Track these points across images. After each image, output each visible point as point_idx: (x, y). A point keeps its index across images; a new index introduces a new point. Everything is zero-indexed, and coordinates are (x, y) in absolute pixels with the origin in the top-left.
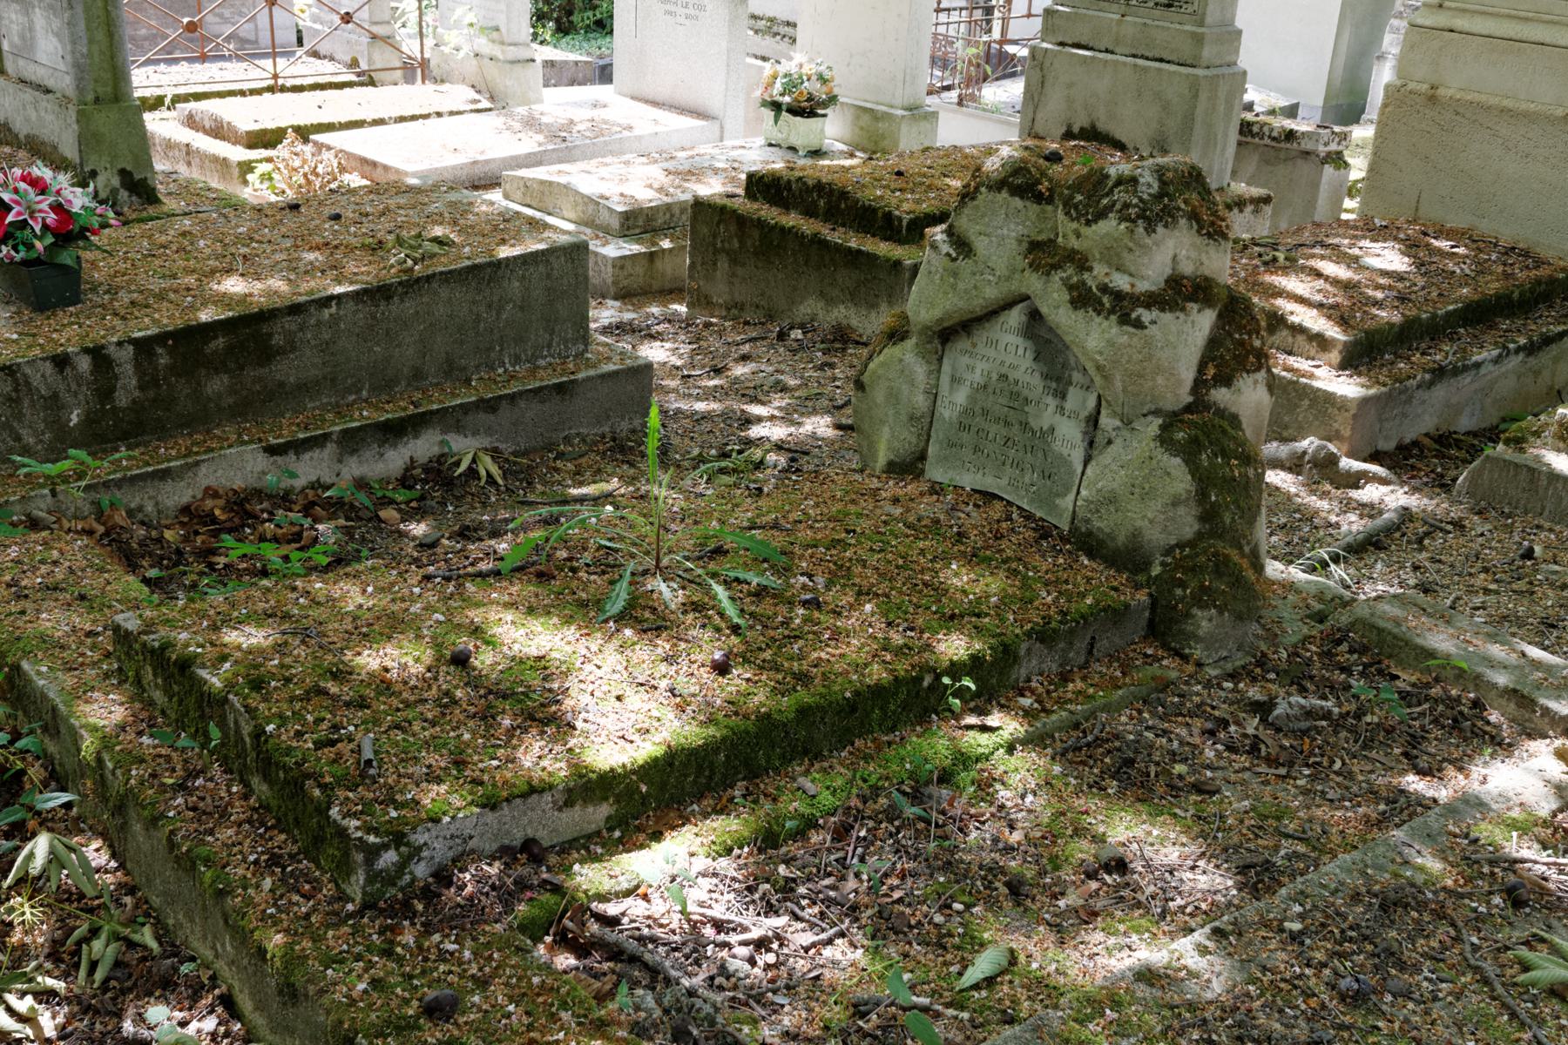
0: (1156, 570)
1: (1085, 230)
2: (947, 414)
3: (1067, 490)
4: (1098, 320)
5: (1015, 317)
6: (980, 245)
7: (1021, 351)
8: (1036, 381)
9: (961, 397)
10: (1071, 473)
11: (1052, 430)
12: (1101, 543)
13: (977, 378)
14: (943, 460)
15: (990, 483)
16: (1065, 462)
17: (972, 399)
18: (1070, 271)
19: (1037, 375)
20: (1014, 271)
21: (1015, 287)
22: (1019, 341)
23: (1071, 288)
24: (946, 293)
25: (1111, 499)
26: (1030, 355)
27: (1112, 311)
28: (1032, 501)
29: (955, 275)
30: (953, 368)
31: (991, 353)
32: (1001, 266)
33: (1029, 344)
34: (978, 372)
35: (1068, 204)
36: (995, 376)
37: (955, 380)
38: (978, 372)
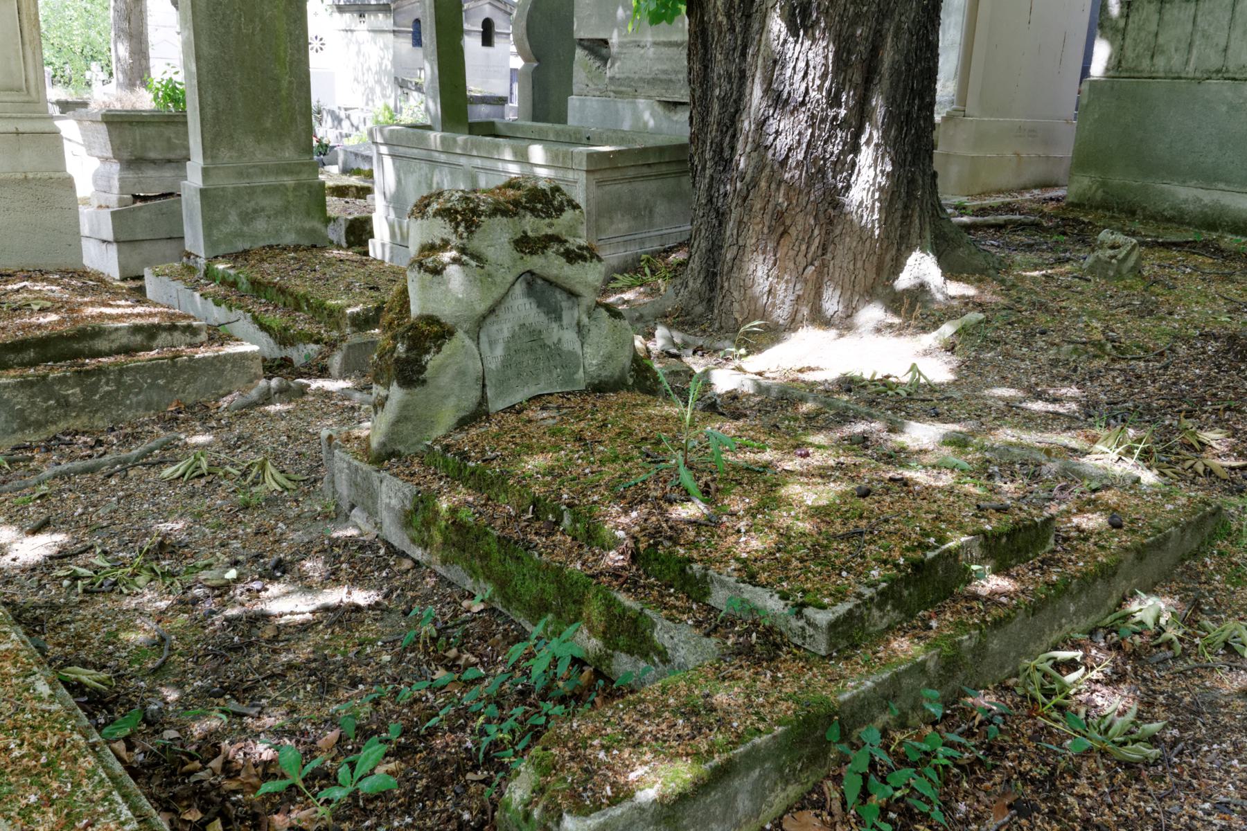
0: (630, 381)
1: (555, 221)
2: (493, 367)
3: (578, 367)
4: (587, 264)
5: (519, 288)
6: (490, 253)
7: (528, 306)
8: (542, 318)
9: (499, 351)
10: (577, 357)
11: (560, 340)
12: (607, 383)
13: (506, 333)
14: (498, 396)
15: (533, 390)
16: (572, 353)
17: (507, 349)
18: (556, 246)
19: (542, 315)
20: (515, 261)
21: (521, 269)
22: (526, 300)
23: (562, 255)
24: (489, 289)
25: (610, 357)
26: (534, 306)
27: (592, 257)
28: (561, 385)
29: (489, 275)
30: (488, 336)
31: (511, 315)
32: (507, 262)
33: (532, 300)
34: (505, 330)
35: (533, 211)
36: (517, 328)
37: (492, 344)
38: (505, 330)
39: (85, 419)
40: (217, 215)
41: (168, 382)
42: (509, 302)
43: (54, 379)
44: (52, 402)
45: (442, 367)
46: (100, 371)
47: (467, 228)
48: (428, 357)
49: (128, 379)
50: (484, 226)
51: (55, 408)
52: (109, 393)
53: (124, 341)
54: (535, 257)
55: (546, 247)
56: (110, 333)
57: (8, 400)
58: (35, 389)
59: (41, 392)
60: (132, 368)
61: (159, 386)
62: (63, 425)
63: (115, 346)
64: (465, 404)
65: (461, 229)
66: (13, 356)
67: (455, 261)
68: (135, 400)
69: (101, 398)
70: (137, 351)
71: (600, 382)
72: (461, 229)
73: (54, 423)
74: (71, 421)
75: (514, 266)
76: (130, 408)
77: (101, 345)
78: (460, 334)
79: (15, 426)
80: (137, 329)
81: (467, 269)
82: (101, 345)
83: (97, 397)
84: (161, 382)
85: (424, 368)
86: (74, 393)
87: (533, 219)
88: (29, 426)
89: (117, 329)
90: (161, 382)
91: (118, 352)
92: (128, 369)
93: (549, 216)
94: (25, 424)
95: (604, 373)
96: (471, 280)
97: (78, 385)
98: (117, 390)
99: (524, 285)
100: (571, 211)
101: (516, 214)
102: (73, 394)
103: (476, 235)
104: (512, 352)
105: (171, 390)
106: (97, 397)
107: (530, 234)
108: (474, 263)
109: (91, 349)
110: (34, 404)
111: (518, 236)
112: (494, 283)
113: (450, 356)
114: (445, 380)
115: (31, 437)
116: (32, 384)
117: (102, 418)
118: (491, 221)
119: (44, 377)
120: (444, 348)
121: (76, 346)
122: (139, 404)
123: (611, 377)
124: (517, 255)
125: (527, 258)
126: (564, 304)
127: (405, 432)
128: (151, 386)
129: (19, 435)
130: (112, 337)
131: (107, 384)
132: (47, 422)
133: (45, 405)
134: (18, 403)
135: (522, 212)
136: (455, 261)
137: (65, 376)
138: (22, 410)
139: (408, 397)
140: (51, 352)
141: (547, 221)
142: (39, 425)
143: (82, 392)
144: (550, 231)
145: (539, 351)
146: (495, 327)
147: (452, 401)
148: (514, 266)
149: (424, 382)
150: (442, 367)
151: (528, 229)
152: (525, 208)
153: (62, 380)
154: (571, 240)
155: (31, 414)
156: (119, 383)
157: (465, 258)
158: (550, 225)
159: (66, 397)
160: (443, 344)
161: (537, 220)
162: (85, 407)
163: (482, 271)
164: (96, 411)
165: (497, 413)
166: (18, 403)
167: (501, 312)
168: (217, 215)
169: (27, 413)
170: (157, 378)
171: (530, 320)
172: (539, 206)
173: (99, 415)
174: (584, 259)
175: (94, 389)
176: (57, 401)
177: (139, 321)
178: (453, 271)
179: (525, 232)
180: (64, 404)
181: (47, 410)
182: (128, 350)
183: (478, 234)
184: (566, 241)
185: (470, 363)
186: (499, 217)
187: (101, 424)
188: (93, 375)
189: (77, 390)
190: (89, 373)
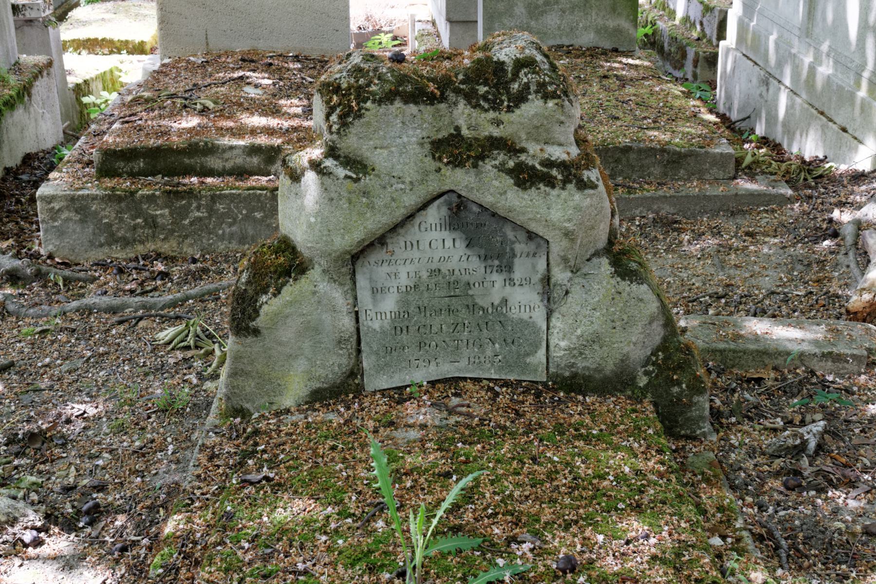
0: (643, 381)
1: (505, 117)
2: (376, 325)
3: (536, 347)
4: (555, 192)
5: (434, 214)
6: (379, 159)
7: (449, 243)
8: (475, 264)
9: (389, 304)
10: (536, 331)
11: (505, 301)
12: (588, 379)
13: (404, 280)
14: (380, 369)
15: (447, 370)
16: (528, 325)
17: (404, 302)
18: (501, 157)
19: (474, 259)
20: (426, 173)
21: (434, 186)
22: (446, 234)
23: (510, 172)
24: (361, 214)
25: (596, 339)
26: (461, 244)
27: (566, 181)
28: (500, 369)
29: (366, 194)
30: (371, 280)
31: (415, 254)
32: (410, 173)
33: (456, 235)
34: (403, 276)
35: (471, 97)
36: (425, 275)
37: (376, 291)
38: (403, 276)
39: (174, 243)
40: (501, 6)
41: (266, 216)
42: (413, 233)
43: (143, 196)
44: (139, 220)
45: (279, 318)
46: (190, 193)
47: (340, 117)
48: (264, 298)
49: (220, 207)
50: (368, 116)
51: (142, 227)
52: (200, 219)
53: (239, 161)
54: (459, 173)
55: (482, 157)
56: (224, 151)
57: (96, 213)
58: (123, 205)
59: (129, 209)
60: (225, 196)
61: (255, 220)
62: (151, 246)
63: (229, 165)
64: (321, 372)
65: (334, 118)
66: (122, 164)
67: (315, 166)
68: (228, 230)
69: (191, 224)
70: (251, 173)
71: (575, 375)
72: (334, 118)
73: (142, 242)
74: (159, 244)
75: (422, 182)
76: (222, 238)
77: (214, 162)
78: (315, 273)
79: (102, 239)
80: (254, 150)
81: (328, 181)
82: (214, 162)
83: (187, 222)
84: (258, 215)
85: (257, 312)
86: (162, 213)
87: (468, 110)
88: (117, 242)
89: (232, 148)
90: (258, 215)
91: (230, 173)
92: (222, 197)
93: (495, 106)
94: (113, 240)
95: (581, 364)
96: (329, 197)
97: (166, 207)
98: (210, 217)
99: (444, 211)
100: (539, 103)
101: (443, 99)
102: (162, 215)
103: (353, 130)
104: (412, 309)
105: (268, 226)
106: (187, 222)
107: (465, 132)
108: (341, 172)
109: (202, 167)
110: (121, 220)
111: (443, 134)
112: (371, 206)
113: (291, 303)
114: (287, 333)
115: (120, 254)
116: (120, 199)
117: (191, 245)
118: (383, 109)
119: (133, 193)
120: (286, 290)
121: (186, 161)
122: (232, 235)
123: (598, 370)
124: (430, 164)
125: (447, 171)
126: (519, 248)
127: (248, 389)
128: (247, 217)
129: (106, 249)
130: (227, 155)
131: (198, 208)
132: (135, 240)
133: (133, 223)
134: (106, 217)
135: (452, 96)
136: (315, 166)
137: (153, 195)
138: (110, 225)
139: (240, 347)
140: (161, 165)
141: (492, 114)
142: (126, 243)
143: (171, 214)
144: (496, 132)
145: (463, 314)
146: (385, 269)
147: (300, 366)
148: (422, 182)
149: (256, 332)
150: (279, 318)
151: (462, 122)
152: (457, 91)
153: (151, 199)
154: (533, 148)
155: (119, 229)
156: (211, 211)
157: (329, 163)
158: (498, 123)
159: (154, 218)
160: (284, 284)
161: (475, 113)
162: (173, 231)
163: (354, 186)
164: (186, 237)
165: (374, 393)
166: (106, 217)
167: (397, 244)
168: (501, 6)
169: (114, 228)
170: (253, 210)
171: (453, 264)
172: (482, 89)
173: (189, 241)
174: (551, 182)
175: (183, 212)
176: (145, 220)
177: (262, 140)
178: (310, 178)
179: (458, 129)
180: (152, 223)
181: (135, 228)
182: (242, 173)
183: (357, 128)
184: (523, 150)
185: (327, 317)
186: (398, 104)
187: (190, 251)
188: (183, 198)
189: (166, 211)
190: (178, 195)
